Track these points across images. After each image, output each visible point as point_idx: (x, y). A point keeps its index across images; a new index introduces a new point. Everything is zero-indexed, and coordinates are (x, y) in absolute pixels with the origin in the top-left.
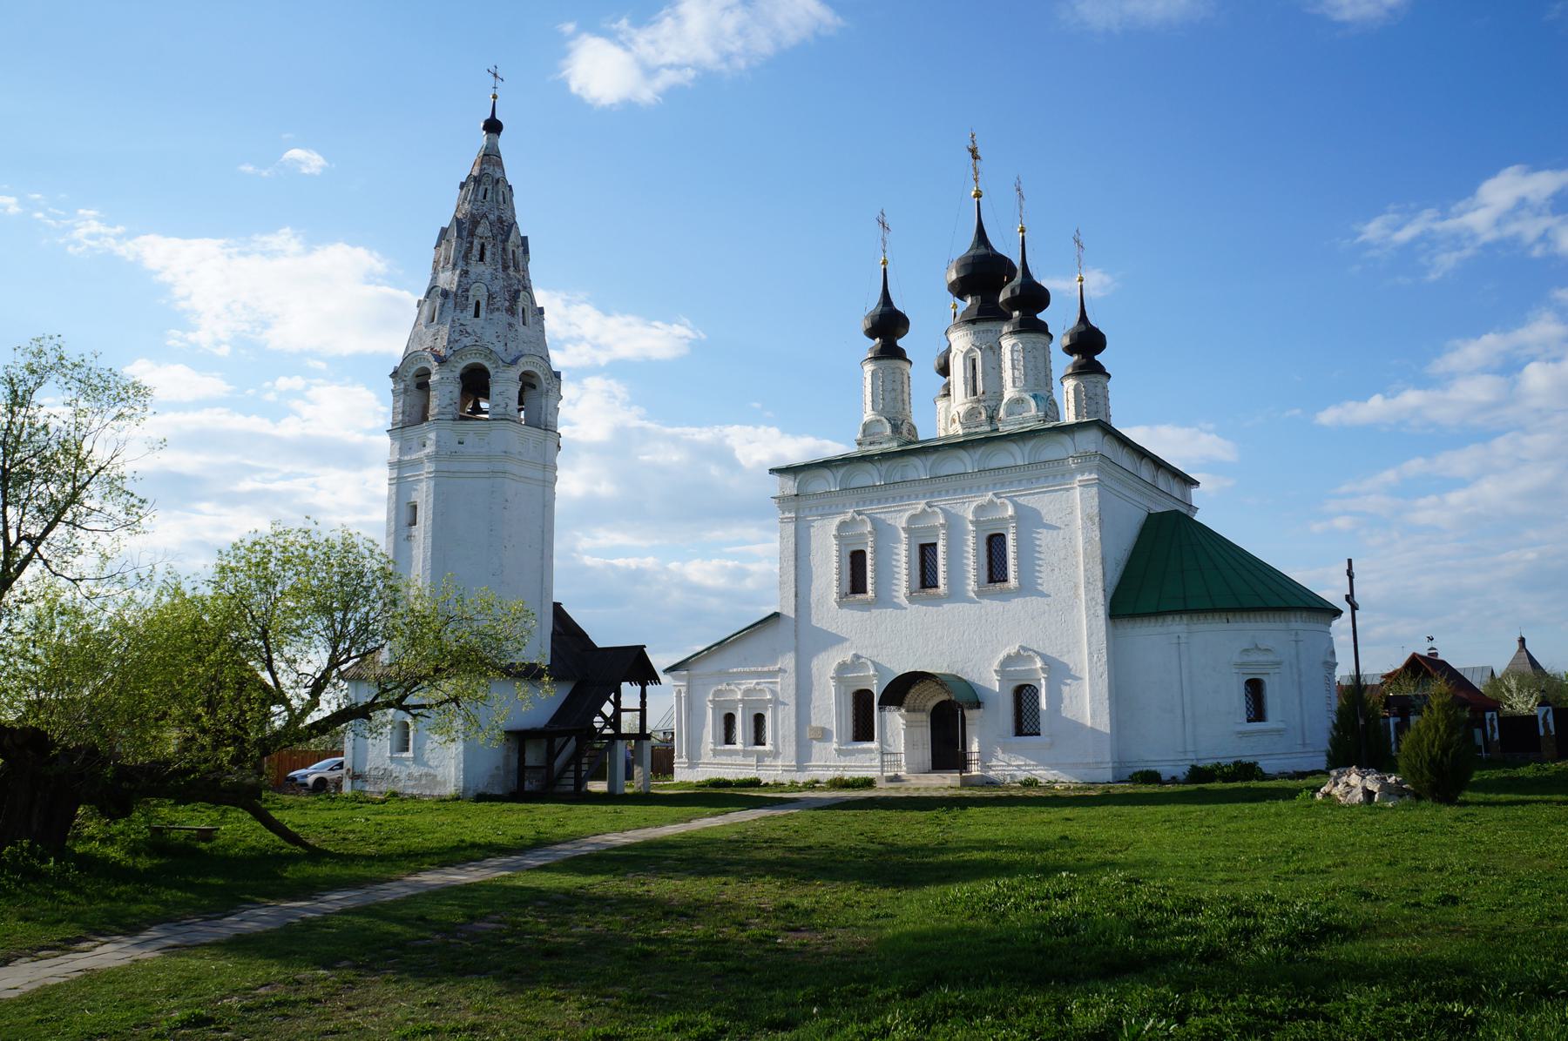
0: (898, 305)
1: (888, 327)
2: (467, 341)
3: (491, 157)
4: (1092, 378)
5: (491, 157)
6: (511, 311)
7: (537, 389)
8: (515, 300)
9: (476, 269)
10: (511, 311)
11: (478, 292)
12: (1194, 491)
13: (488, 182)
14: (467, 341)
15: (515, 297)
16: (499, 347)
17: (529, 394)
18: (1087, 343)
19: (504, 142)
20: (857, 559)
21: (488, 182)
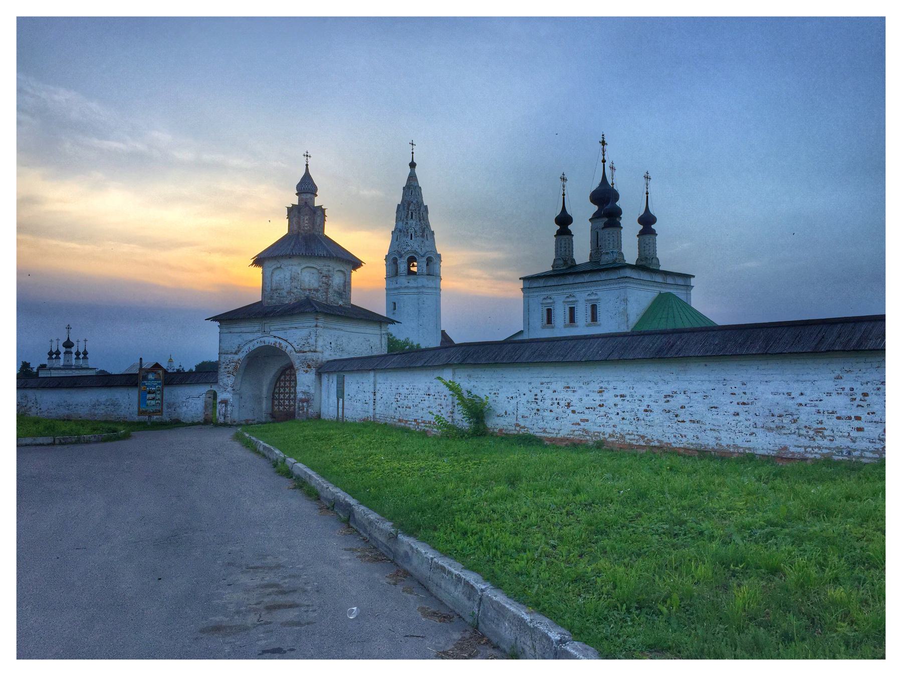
0: (569, 212)
1: (564, 220)
2: (409, 248)
3: (412, 177)
4: (647, 238)
5: (412, 177)
6: (423, 236)
7: (432, 261)
8: (426, 233)
9: (410, 222)
10: (423, 236)
11: (411, 231)
12: (692, 279)
13: (412, 188)
14: (409, 248)
15: (423, 231)
16: (419, 250)
17: (430, 264)
18: (647, 221)
19: (417, 170)
20: (549, 311)
21: (412, 188)
